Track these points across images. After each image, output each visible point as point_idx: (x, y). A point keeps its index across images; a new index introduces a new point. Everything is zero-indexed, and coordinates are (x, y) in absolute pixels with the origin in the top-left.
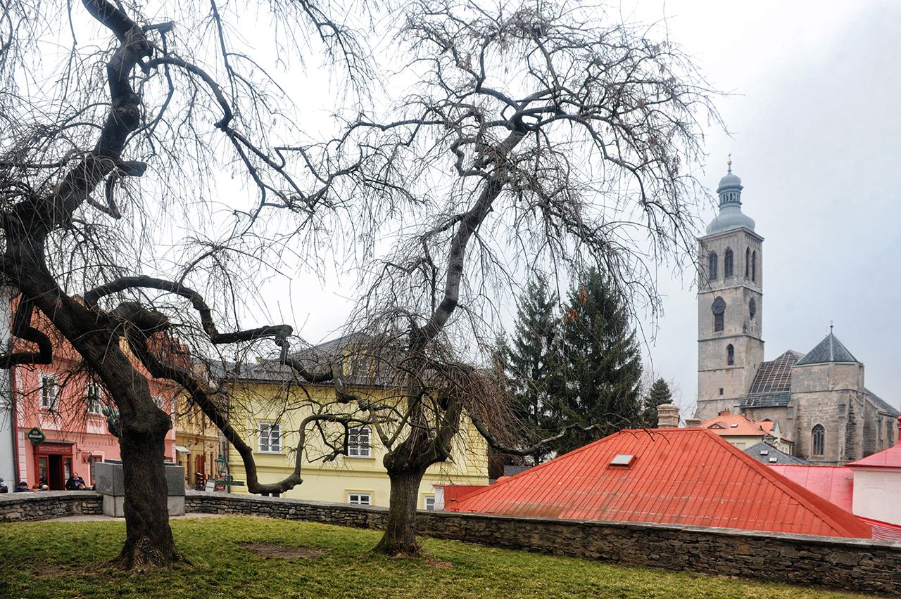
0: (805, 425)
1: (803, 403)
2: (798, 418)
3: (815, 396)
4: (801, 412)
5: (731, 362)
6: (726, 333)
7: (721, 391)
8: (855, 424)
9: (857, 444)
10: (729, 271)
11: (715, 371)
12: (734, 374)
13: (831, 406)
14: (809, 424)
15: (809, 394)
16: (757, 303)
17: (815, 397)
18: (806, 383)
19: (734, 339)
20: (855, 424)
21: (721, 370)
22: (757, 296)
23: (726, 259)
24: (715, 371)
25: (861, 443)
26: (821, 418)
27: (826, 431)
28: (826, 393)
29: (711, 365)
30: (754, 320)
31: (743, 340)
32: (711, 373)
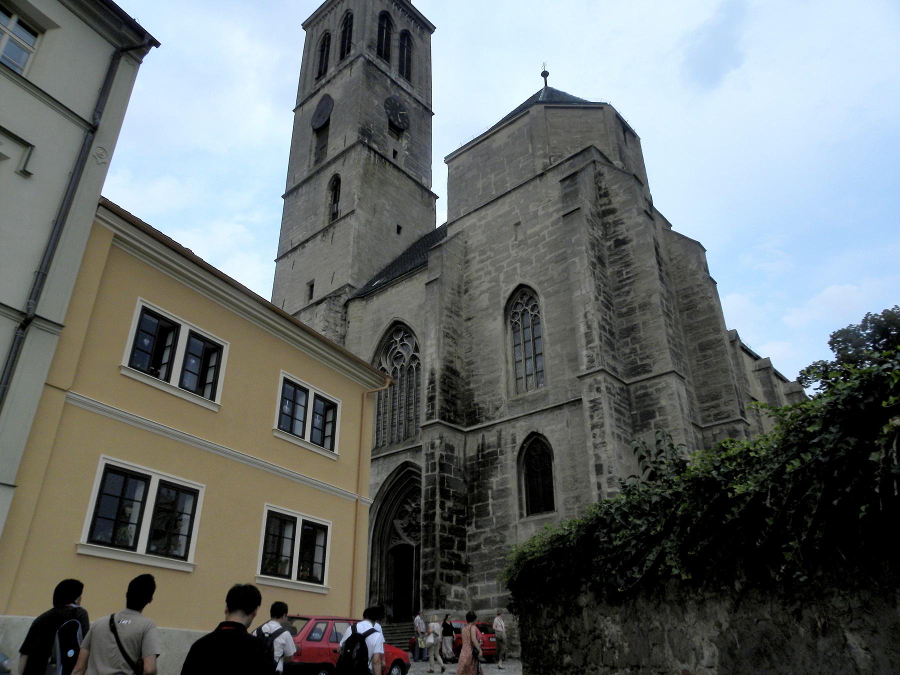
0: (484, 301)
1: (476, 239)
2: (463, 289)
3: (503, 207)
4: (475, 266)
5: (334, 216)
6: (331, 153)
7: (312, 287)
8: (624, 242)
9: (644, 306)
10: (345, 50)
11: (303, 244)
12: (336, 236)
13: (550, 215)
14: (494, 295)
15: (490, 213)
16: (413, 119)
17: (506, 208)
18: (480, 185)
19: (341, 160)
20: (624, 242)
21: (314, 236)
22: (414, 105)
23: (344, 33)
24: (303, 244)
25: (656, 299)
26: (526, 262)
27: (542, 300)
28: (530, 187)
29: (298, 237)
30: (404, 143)
31: (360, 154)
32: (298, 252)
